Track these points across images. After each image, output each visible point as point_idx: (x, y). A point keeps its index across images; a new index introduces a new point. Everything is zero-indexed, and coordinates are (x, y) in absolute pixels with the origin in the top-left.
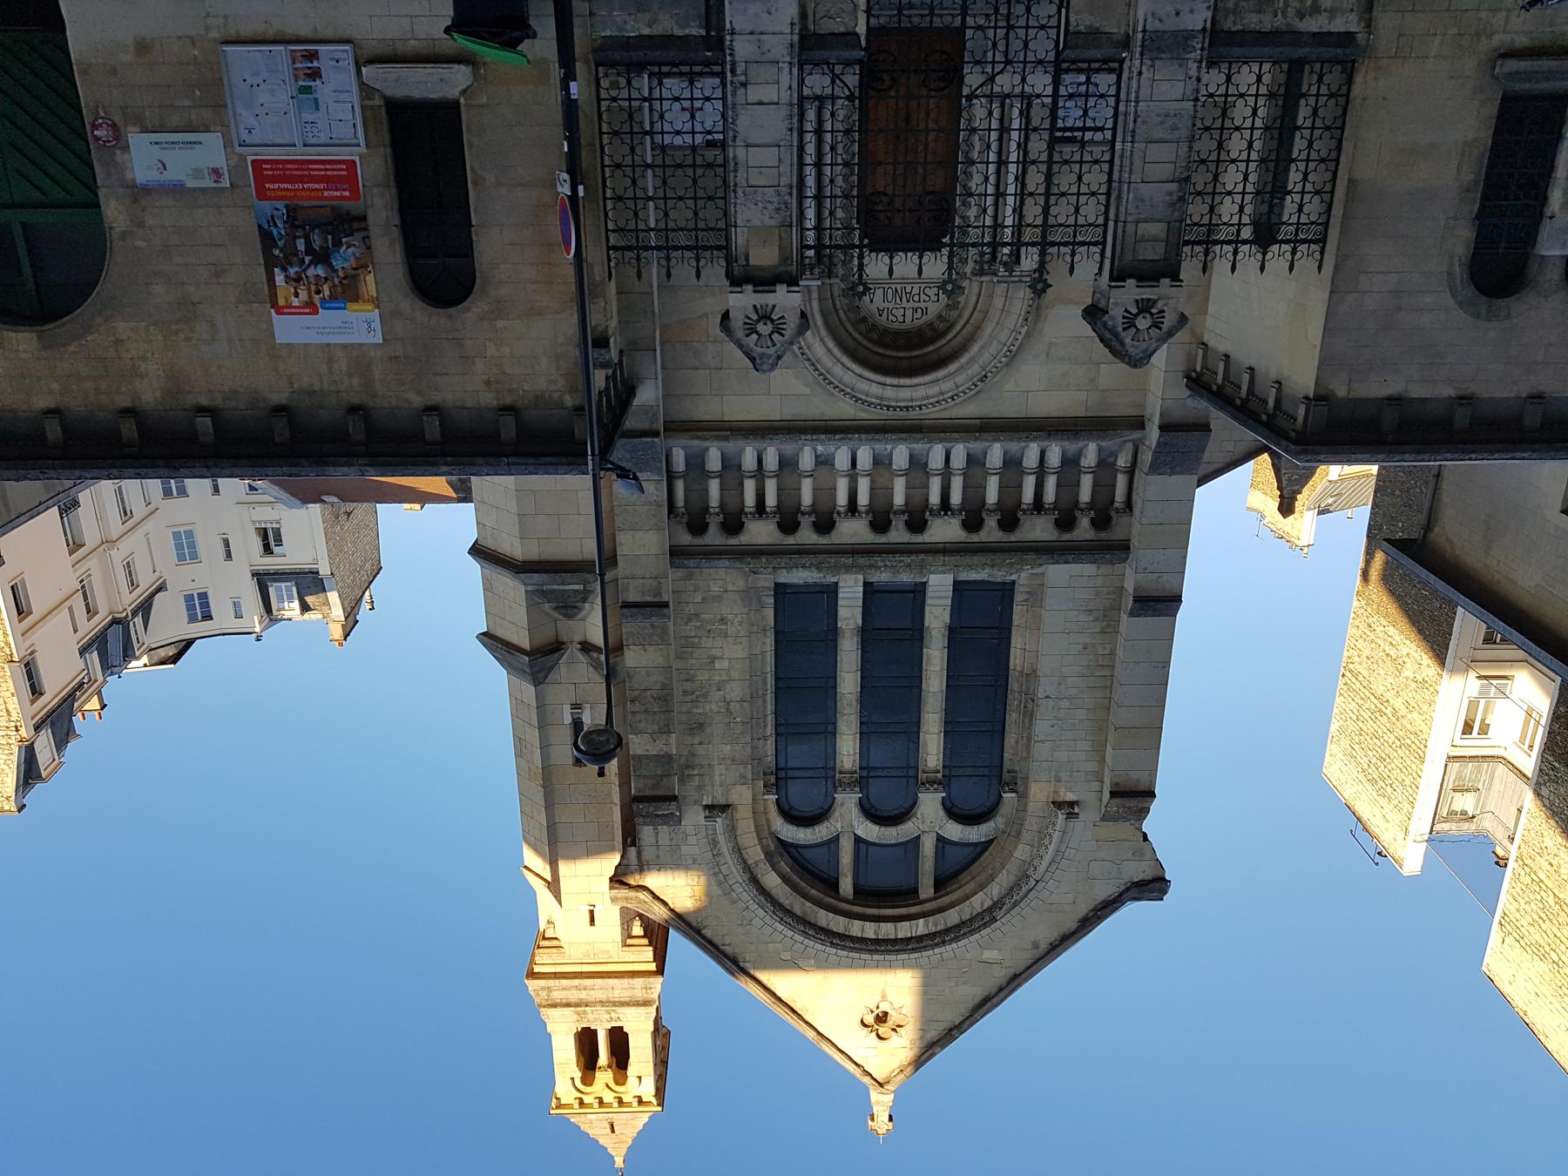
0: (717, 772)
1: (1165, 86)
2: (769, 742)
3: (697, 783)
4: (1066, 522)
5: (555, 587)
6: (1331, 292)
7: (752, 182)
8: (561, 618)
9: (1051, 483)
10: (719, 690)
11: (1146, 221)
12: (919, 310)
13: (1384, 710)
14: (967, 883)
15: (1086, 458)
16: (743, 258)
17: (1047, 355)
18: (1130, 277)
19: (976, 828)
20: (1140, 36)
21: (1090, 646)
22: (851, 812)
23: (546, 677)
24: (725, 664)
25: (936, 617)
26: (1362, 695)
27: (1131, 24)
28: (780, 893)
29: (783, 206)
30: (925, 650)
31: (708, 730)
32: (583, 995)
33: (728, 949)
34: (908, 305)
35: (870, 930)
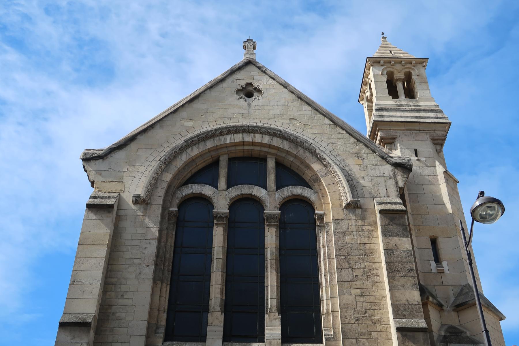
0: (353, 227)
8: (457, 327)
10: (356, 276)
19: (194, 192)
21: (119, 297)
22: (270, 203)
23: (462, 290)
25: (217, 319)
28: (312, 159)
30: (224, 298)
32: (417, 114)
33: (341, 131)
35: (258, 138)
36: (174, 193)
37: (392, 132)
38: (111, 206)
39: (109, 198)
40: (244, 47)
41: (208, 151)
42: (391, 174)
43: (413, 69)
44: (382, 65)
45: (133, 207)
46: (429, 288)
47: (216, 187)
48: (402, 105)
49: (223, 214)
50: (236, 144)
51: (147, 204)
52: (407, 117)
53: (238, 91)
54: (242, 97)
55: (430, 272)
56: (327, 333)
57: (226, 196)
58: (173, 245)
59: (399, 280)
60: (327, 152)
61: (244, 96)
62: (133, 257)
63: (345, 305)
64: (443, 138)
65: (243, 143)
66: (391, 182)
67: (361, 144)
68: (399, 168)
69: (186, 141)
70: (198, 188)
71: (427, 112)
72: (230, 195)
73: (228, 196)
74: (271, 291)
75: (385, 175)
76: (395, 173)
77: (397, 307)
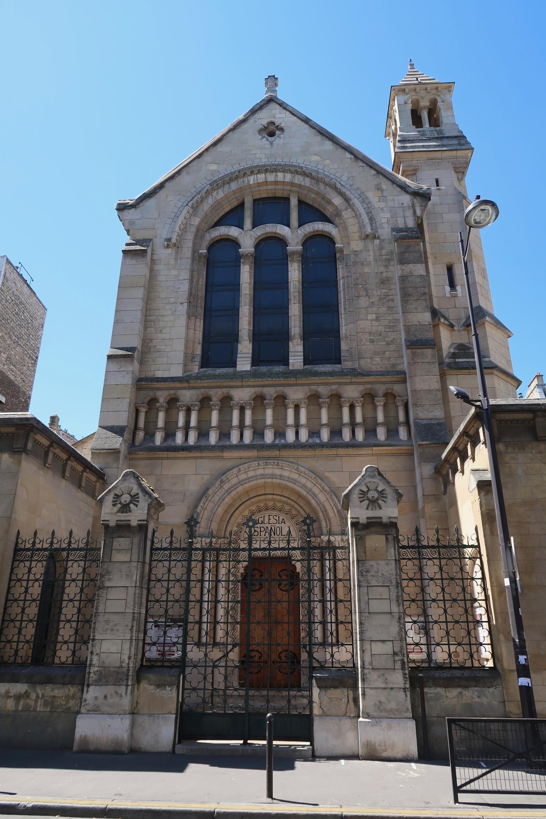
1: (114, 649)
2: (341, 276)
3: (383, 251)
4: (173, 402)
6: (10, 517)
7: (386, 589)
8: (466, 344)
10: (372, 302)
11: (125, 562)
12: (260, 522)
13: (16, 338)
15: (162, 437)
16: (389, 539)
17: (185, 495)
19: (221, 234)
20: (130, 683)
24: (370, 317)
26: (27, 347)
29: (364, 573)
30: (252, 329)
31: (378, 280)
33: (361, 164)
34: (265, 526)
35: (280, 176)
36: (202, 237)
40: (266, 84)
43: (439, 95)
46: (442, 311)
47: (242, 228)
50: (259, 184)
53: (260, 131)
54: (264, 137)
55: (444, 297)
58: (204, 284)
60: (347, 186)
61: (266, 136)
62: (168, 296)
64: (465, 165)
65: (266, 183)
66: (409, 213)
70: (225, 230)
71: (451, 139)
72: (255, 235)
75: (403, 205)
76: (413, 202)
77: (409, 328)
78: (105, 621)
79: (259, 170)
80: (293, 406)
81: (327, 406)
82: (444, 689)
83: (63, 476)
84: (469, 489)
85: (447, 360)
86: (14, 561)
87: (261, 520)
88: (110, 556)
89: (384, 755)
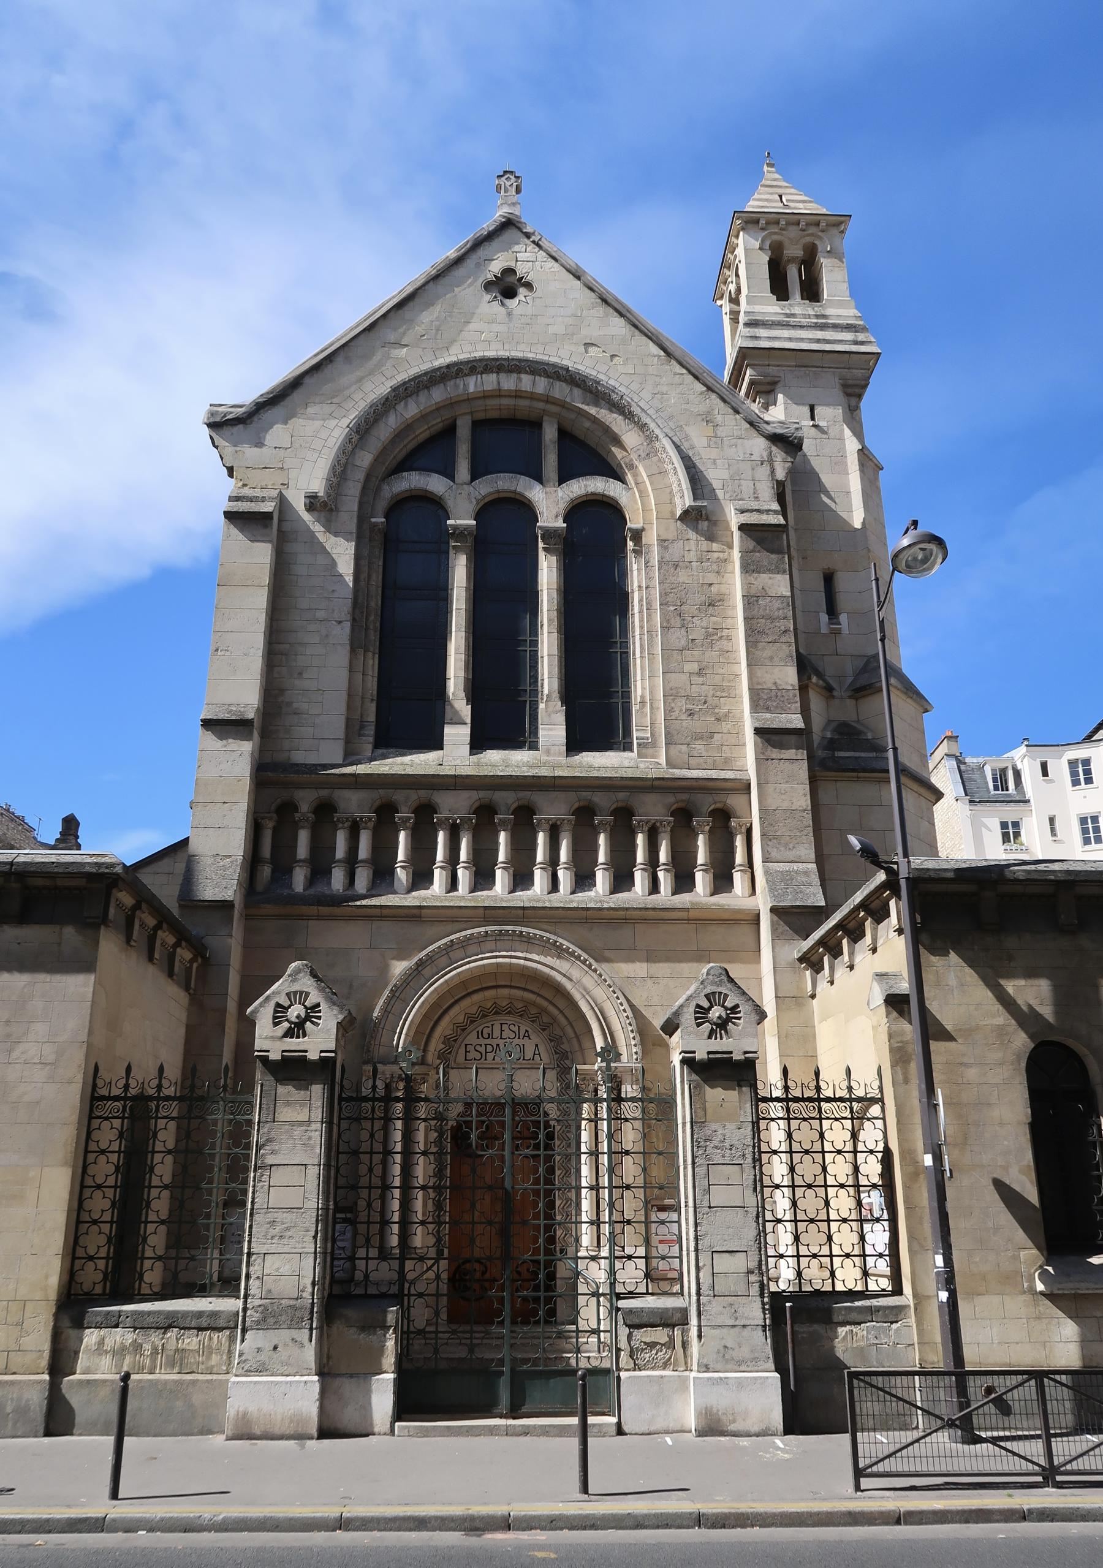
4: (325, 811)
5: (863, 755)
8: (853, 724)
9: (340, 852)
11: (301, 1123)
14: (422, 433)
15: (305, 877)
17: (351, 986)
18: (313, 1062)
19: (413, 487)
22: (548, 507)
27: (326, 1335)
29: (702, 1144)
30: (470, 677)
32: (820, 334)
34: (494, 1042)
35: (526, 382)
36: (378, 489)
37: (772, 370)
38: (266, 517)
39: (263, 499)
41: (434, 407)
42: (765, 454)
43: (820, 238)
44: (763, 229)
45: (306, 516)
47: (452, 478)
48: (793, 315)
49: (465, 529)
50: (486, 396)
51: (331, 510)
52: (802, 340)
53: (488, 286)
55: (817, 632)
56: (641, 734)
57: (470, 494)
58: (380, 584)
59: (764, 649)
60: (651, 412)
63: (671, 689)
64: (863, 383)
65: (499, 394)
67: (714, 396)
68: (779, 444)
69: (395, 389)
70: (419, 480)
73: (473, 496)
74: (550, 665)
75: (753, 458)
78: (269, 1223)
79: (486, 365)
80: (547, 827)
81: (609, 829)
82: (824, 1325)
83: (151, 959)
84: (868, 1004)
85: (820, 753)
86: (91, 1118)
87: (486, 1031)
88: (272, 1113)
89: (732, 1427)
